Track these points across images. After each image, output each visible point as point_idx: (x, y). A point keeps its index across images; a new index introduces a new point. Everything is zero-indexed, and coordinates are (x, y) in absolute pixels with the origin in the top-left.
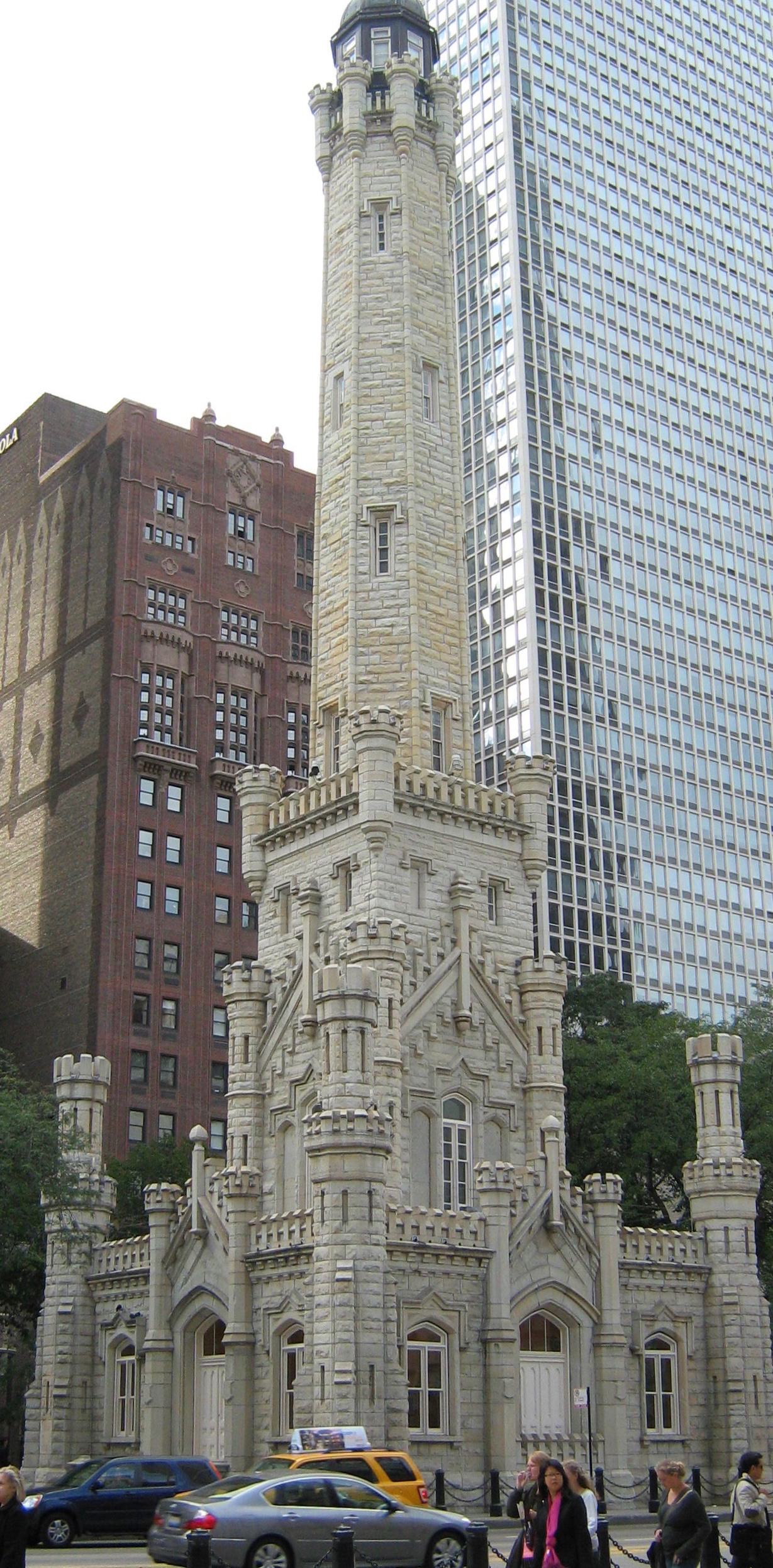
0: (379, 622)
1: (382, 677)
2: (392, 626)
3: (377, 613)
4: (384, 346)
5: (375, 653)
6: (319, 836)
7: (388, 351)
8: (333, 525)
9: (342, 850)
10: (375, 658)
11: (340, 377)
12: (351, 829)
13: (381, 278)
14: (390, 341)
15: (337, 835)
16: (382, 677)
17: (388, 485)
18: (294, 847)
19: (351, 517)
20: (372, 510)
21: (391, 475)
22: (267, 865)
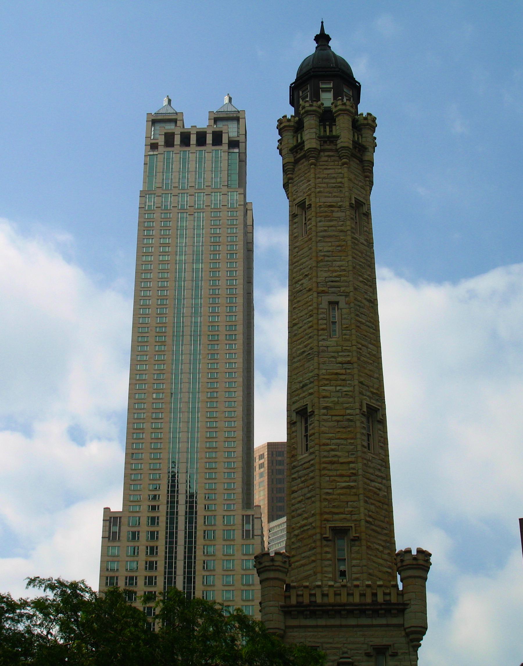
0: (373, 484)
1: (377, 522)
2: (379, 489)
3: (373, 477)
4: (365, 299)
5: (372, 504)
6: (352, 621)
7: (367, 303)
8: (338, 403)
9: (380, 638)
10: (372, 507)
11: (334, 304)
12: (387, 625)
13: (362, 253)
14: (368, 298)
15: (372, 626)
16: (377, 522)
17: (373, 393)
18: (321, 622)
19: (357, 405)
20: (369, 406)
21: (373, 387)
22: (286, 627)
